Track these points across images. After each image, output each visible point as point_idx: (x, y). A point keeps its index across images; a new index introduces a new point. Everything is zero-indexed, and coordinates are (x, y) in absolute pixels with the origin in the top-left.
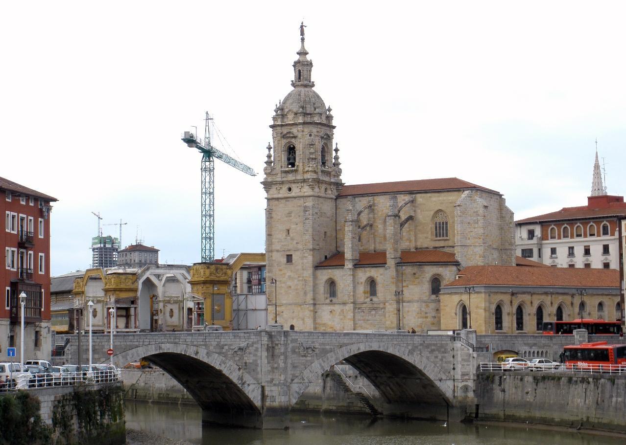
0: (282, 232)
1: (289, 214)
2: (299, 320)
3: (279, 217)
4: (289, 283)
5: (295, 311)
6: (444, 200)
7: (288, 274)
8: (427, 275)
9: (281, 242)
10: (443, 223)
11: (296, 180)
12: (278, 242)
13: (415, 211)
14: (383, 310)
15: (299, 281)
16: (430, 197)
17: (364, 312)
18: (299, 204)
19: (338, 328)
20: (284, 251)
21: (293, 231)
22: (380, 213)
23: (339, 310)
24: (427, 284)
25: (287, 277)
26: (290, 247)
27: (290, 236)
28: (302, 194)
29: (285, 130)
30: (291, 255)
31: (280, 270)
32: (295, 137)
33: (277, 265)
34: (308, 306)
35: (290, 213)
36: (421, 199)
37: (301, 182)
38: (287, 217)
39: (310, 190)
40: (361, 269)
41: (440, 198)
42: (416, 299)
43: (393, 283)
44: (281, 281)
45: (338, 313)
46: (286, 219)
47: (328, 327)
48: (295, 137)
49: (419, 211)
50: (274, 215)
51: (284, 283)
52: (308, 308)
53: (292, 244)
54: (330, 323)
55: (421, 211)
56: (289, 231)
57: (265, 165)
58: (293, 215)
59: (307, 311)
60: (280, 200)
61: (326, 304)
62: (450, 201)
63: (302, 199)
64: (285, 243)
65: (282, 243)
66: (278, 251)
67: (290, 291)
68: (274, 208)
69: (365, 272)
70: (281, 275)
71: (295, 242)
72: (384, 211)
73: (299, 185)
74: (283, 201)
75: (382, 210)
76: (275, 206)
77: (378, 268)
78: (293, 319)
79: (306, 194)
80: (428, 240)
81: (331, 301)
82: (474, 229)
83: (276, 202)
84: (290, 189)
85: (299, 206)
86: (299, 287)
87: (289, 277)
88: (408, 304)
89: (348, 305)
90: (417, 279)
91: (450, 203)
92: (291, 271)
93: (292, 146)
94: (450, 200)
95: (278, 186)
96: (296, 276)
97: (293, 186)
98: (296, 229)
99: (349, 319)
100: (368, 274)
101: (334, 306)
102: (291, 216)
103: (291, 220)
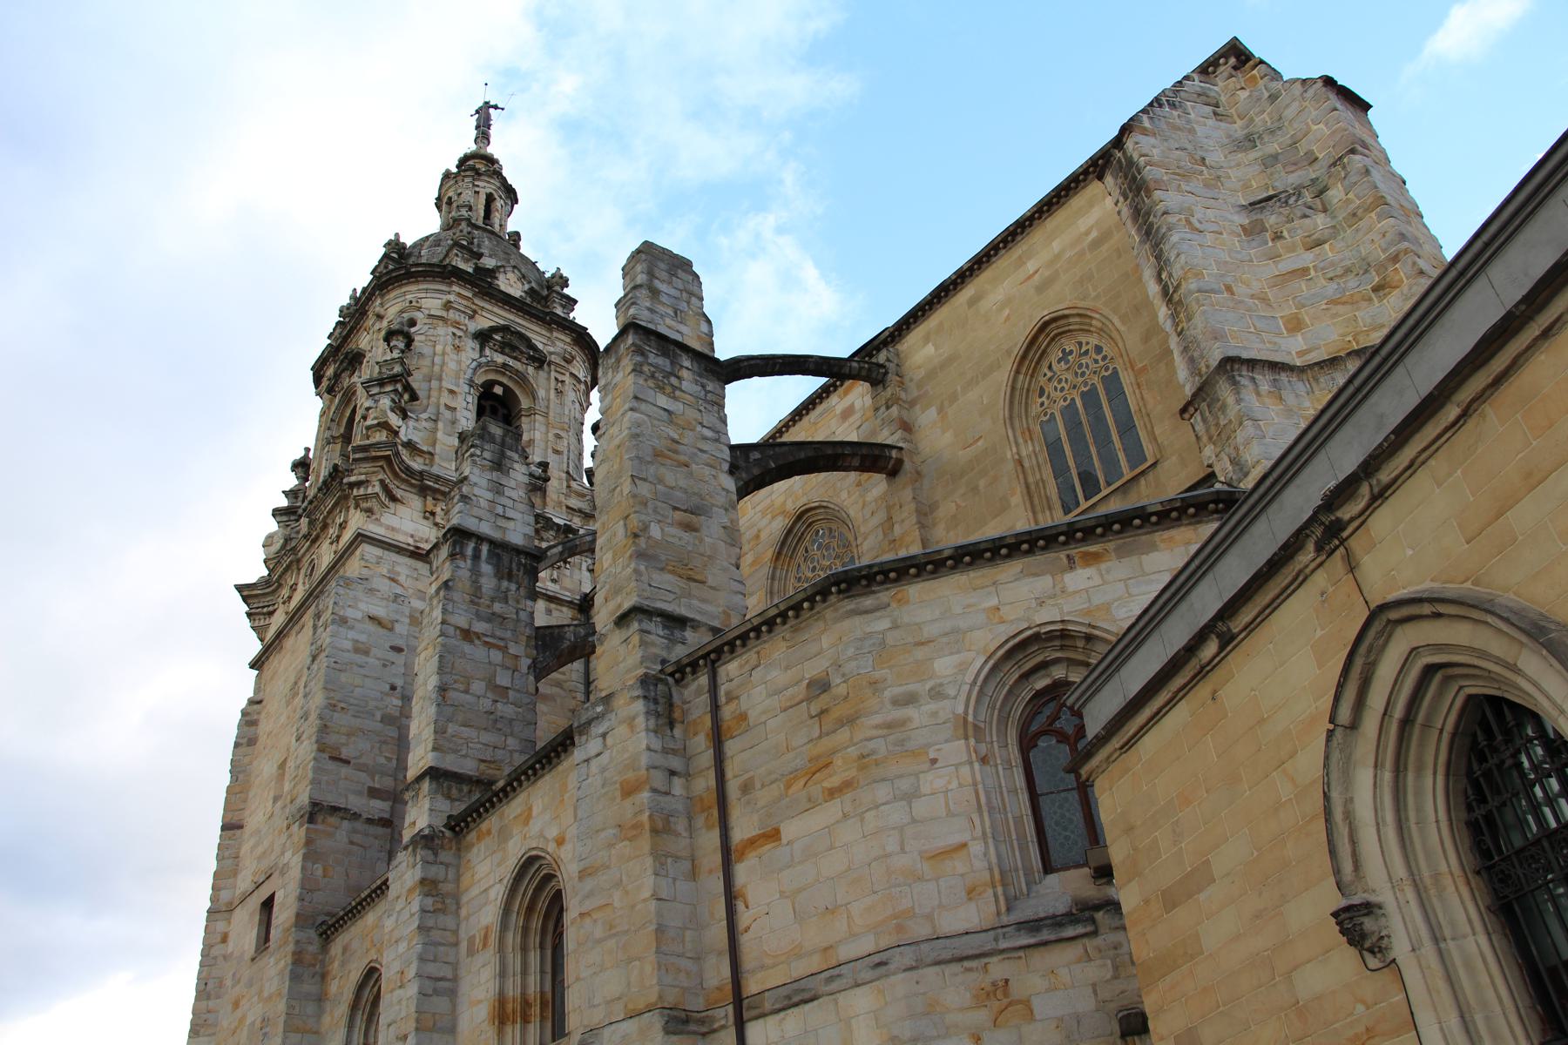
6: (1057, 257)
8: (944, 666)
10: (1090, 397)
13: (906, 427)
16: (973, 302)
24: (956, 750)
36: (930, 349)
41: (1031, 266)
42: (866, 945)
43: (627, 831)
49: (932, 413)
50: (264, 727)
55: (941, 410)
57: (272, 526)
62: (1094, 234)
69: (504, 835)
72: (763, 536)
82: (1307, 258)
88: (792, 1022)
90: (843, 735)
91: (1096, 244)
94: (1087, 233)
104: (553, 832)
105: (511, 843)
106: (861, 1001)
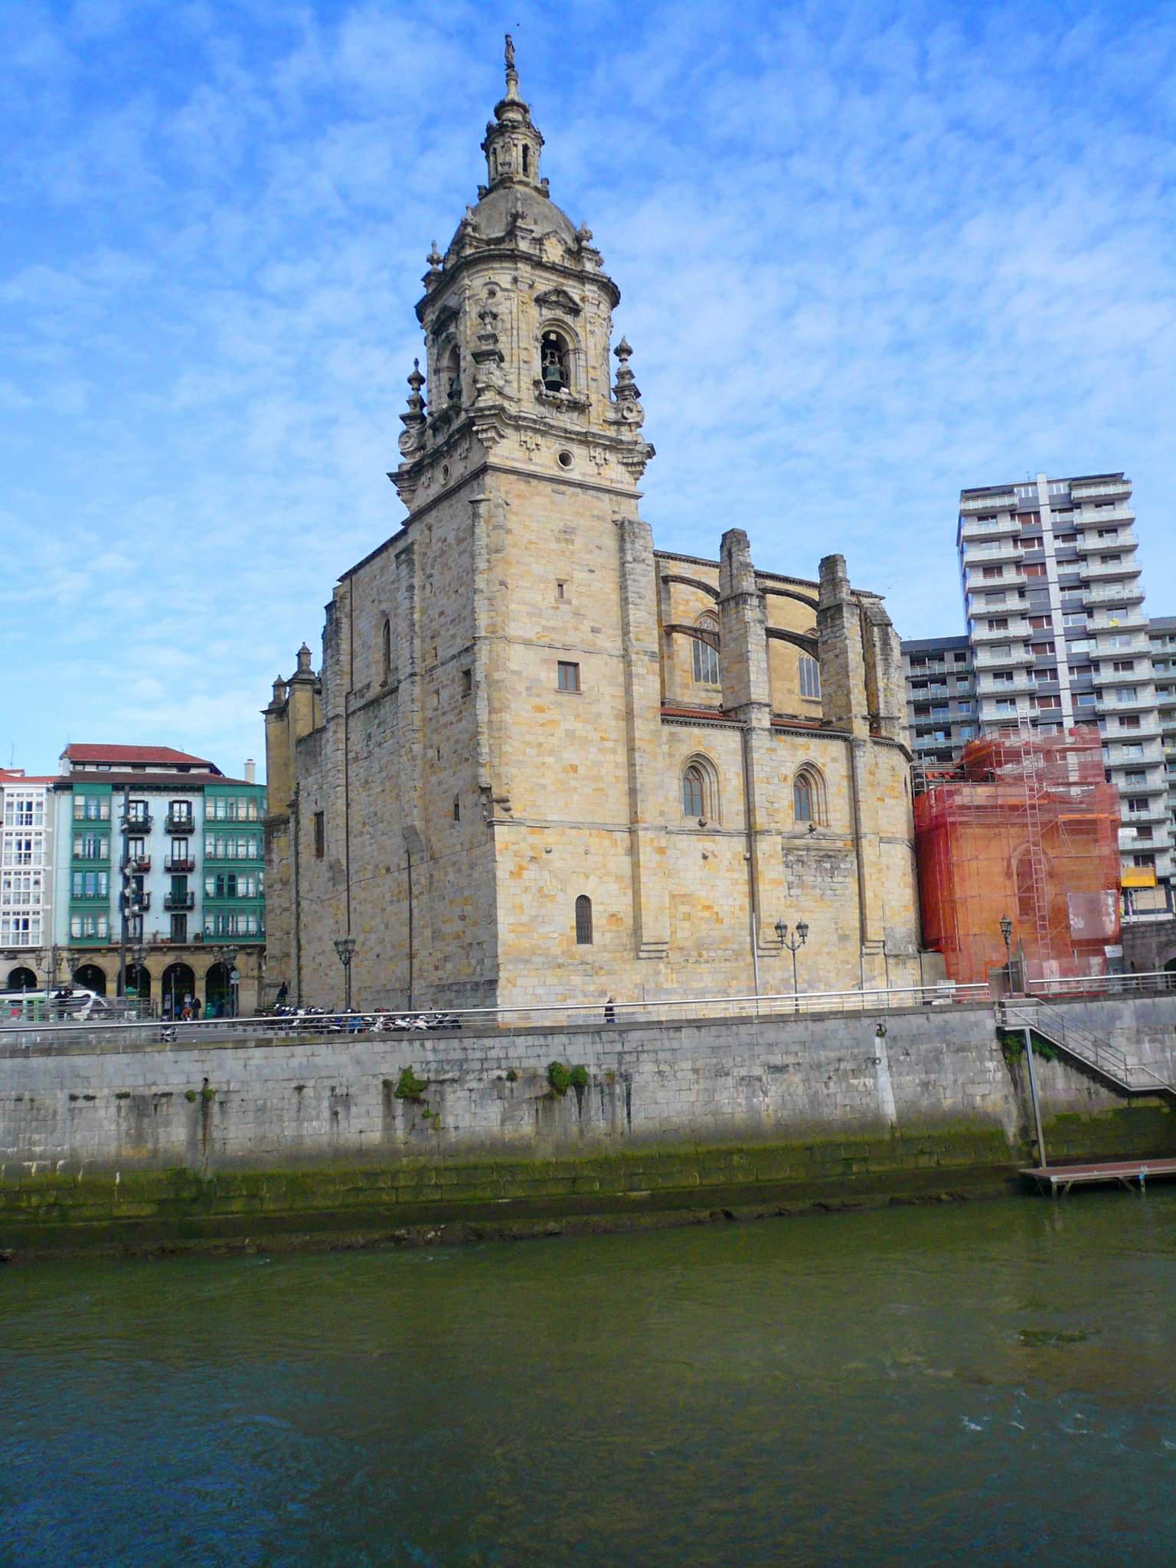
0: (542, 586)
1: (567, 534)
2: (605, 879)
3: (533, 537)
4: (570, 756)
5: (593, 849)
7: (564, 726)
9: (540, 617)
11: (594, 435)
12: (528, 614)
14: (848, 859)
15: (601, 751)
17: (803, 862)
18: (596, 512)
19: (726, 908)
20: (550, 647)
21: (582, 589)
22: (682, 608)
23: (729, 855)
25: (560, 732)
26: (572, 638)
27: (569, 603)
28: (606, 484)
29: (545, 283)
30: (576, 665)
31: (540, 709)
32: (575, 311)
33: (528, 689)
34: (650, 834)
35: (567, 534)
37: (606, 448)
38: (558, 540)
39: (628, 478)
40: (783, 737)
44: (540, 745)
45: (726, 863)
46: (554, 545)
47: (700, 907)
48: (575, 311)
51: (551, 753)
52: (652, 840)
53: (577, 629)
54: (703, 893)
56: (560, 586)
58: (579, 541)
59: (649, 849)
60: (534, 482)
61: (690, 832)
63: (606, 497)
64: (552, 623)
65: (544, 623)
66: (528, 643)
67: (573, 783)
68: (515, 502)
69: (794, 747)
70: (542, 725)
71: (586, 626)
72: (691, 604)
73: (598, 452)
74: (547, 488)
75: (688, 601)
76: (518, 496)
77: (826, 741)
78: (587, 876)
79: (618, 486)
80: (793, 696)
81: (702, 825)
83: (521, 486)
84: (565, 459)
85: (599, 518)
86: (603, 772)
87: (570, 734)
89: (768, 838)
92: (577, 716)
93: (553, 337)
95: (530, 438)
96: (595, 736)
97: (578, 451)
98: (589, 586)
99: (774, 881)
100: (801, 756)
101: (714, 841)
102: (572, 542)
103: (572, 553)
104: (822, 761)
105: (799, 753)
106: (898, 847)
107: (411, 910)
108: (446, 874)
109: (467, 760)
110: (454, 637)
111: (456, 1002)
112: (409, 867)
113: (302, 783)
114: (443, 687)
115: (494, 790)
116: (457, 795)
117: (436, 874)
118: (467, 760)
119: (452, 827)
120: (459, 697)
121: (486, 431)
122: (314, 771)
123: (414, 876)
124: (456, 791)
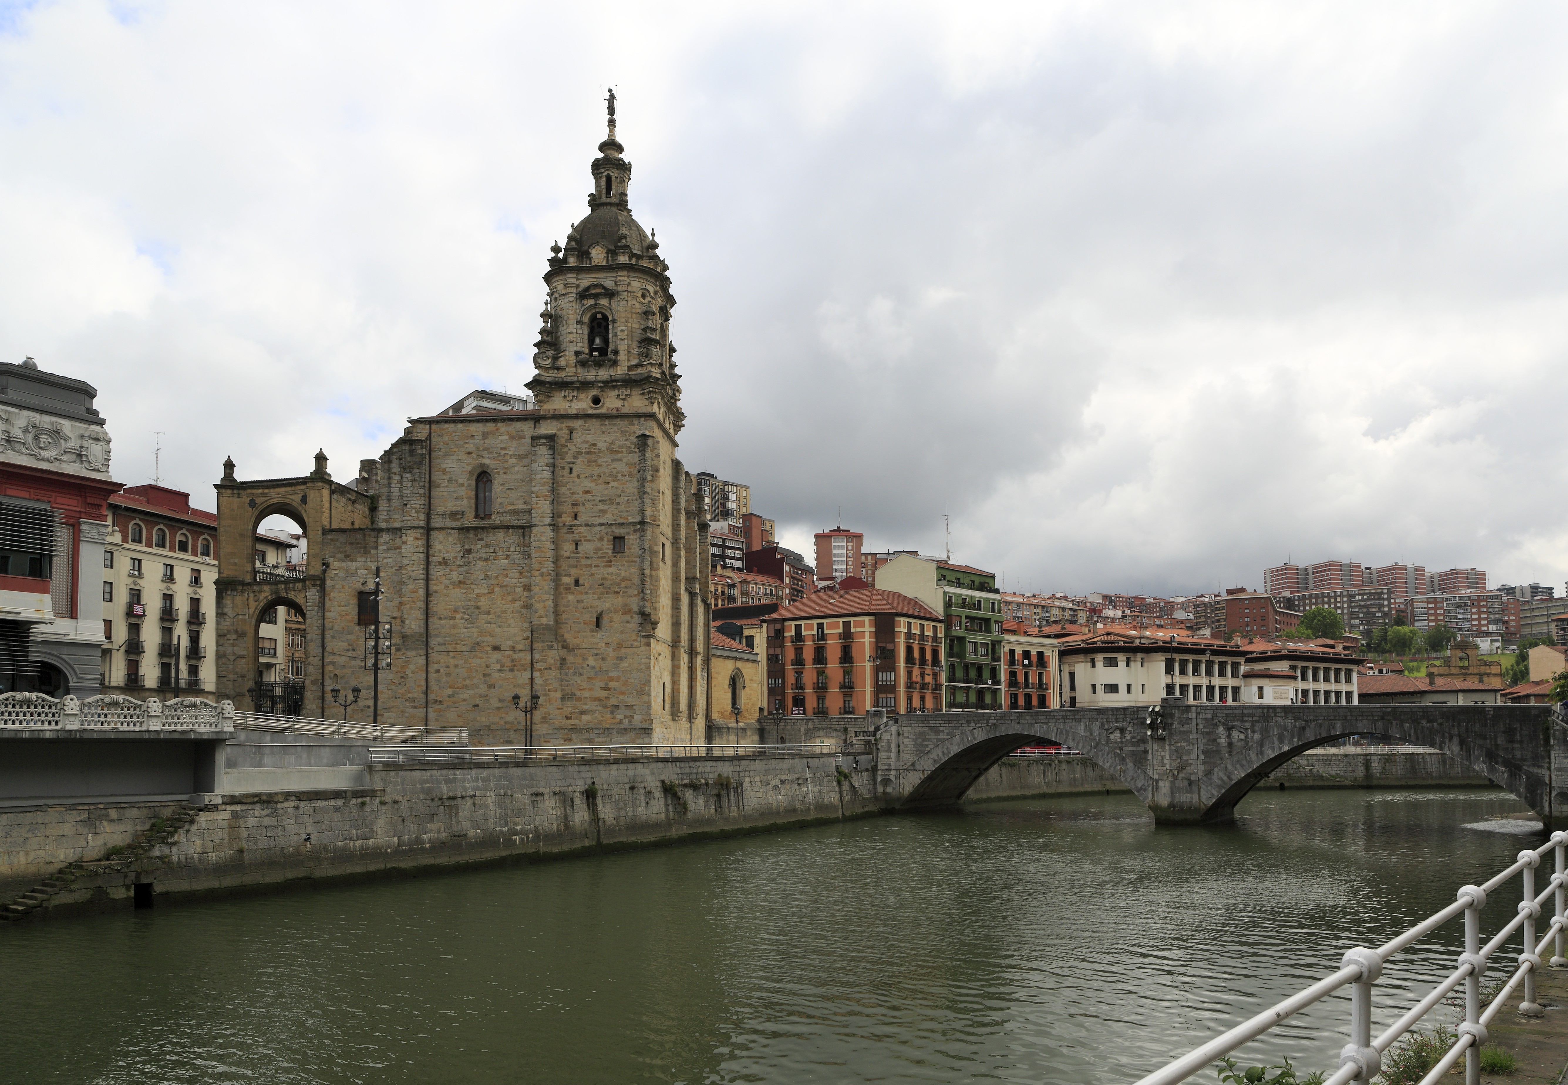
107: (532, 679)
108: (585, 659)
109: (617, 593)
110: (603, 512)
111: (596, 740)
112: (532, 650)
113: (335, 564)
114: (586, 540)
115: (652, 616)
116: (601, 614)
117: (570, 659)
118: (617, 593)
119: (592, 631)
120: (610, 552)
121: (656, 393)
122: (359, 559)
123: (537, 656)
124: (599, 610)
